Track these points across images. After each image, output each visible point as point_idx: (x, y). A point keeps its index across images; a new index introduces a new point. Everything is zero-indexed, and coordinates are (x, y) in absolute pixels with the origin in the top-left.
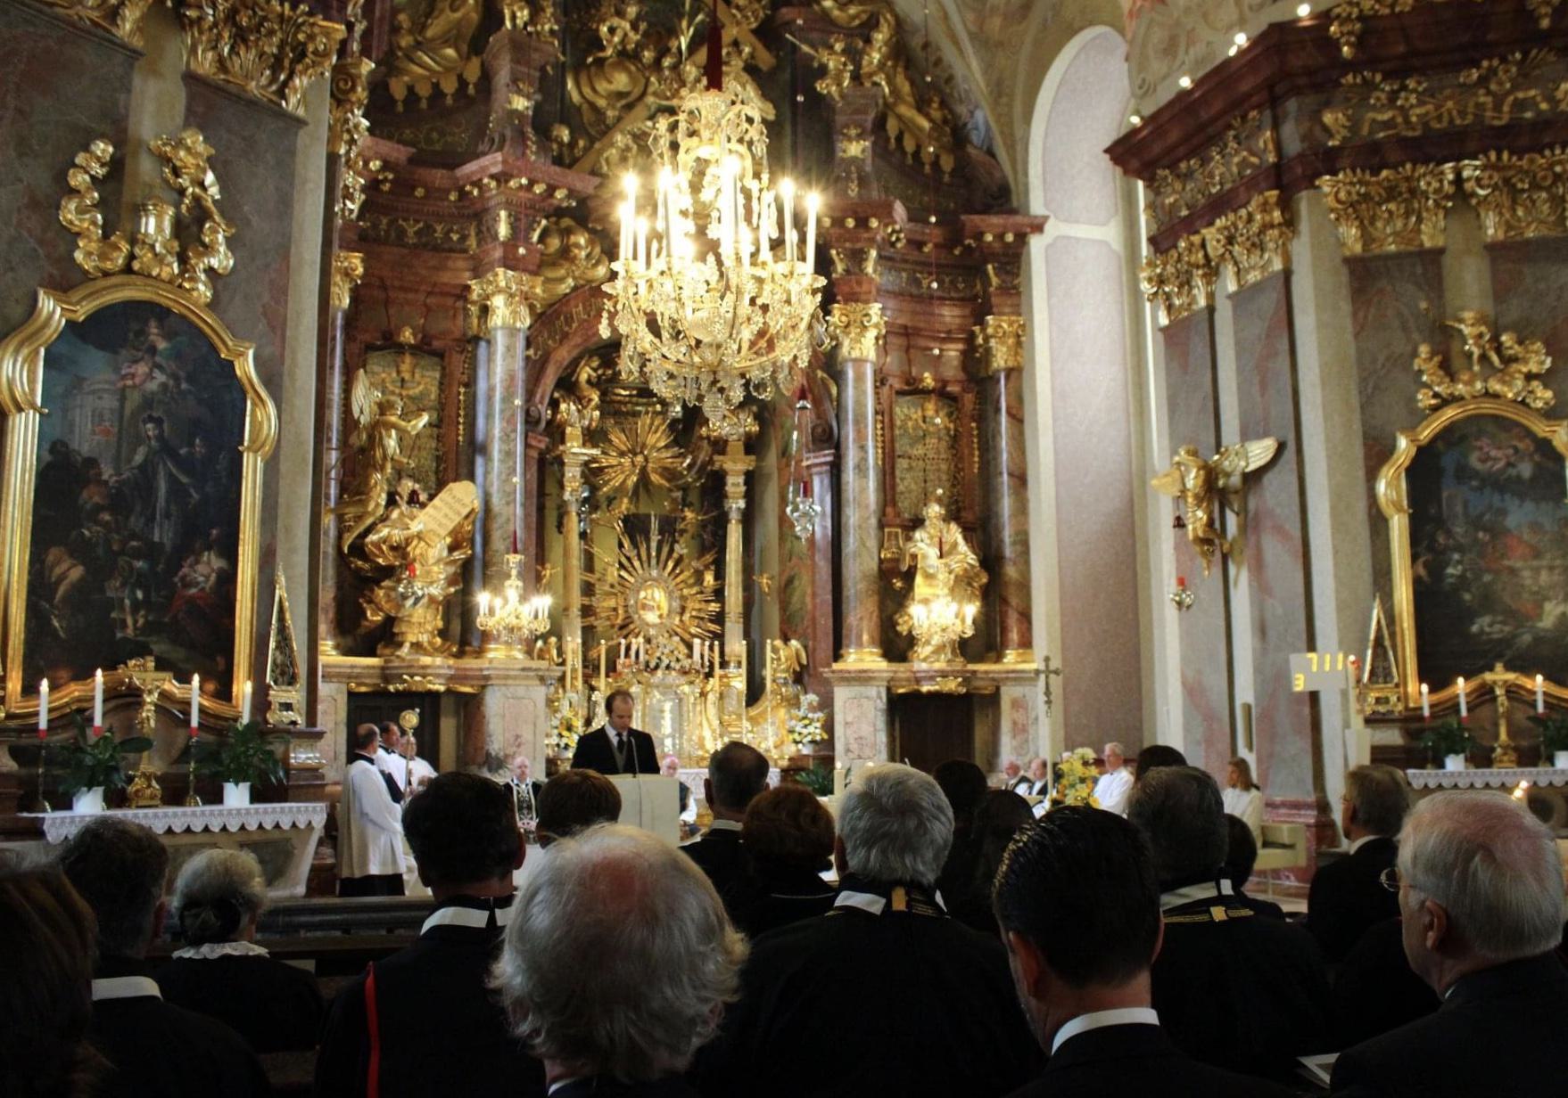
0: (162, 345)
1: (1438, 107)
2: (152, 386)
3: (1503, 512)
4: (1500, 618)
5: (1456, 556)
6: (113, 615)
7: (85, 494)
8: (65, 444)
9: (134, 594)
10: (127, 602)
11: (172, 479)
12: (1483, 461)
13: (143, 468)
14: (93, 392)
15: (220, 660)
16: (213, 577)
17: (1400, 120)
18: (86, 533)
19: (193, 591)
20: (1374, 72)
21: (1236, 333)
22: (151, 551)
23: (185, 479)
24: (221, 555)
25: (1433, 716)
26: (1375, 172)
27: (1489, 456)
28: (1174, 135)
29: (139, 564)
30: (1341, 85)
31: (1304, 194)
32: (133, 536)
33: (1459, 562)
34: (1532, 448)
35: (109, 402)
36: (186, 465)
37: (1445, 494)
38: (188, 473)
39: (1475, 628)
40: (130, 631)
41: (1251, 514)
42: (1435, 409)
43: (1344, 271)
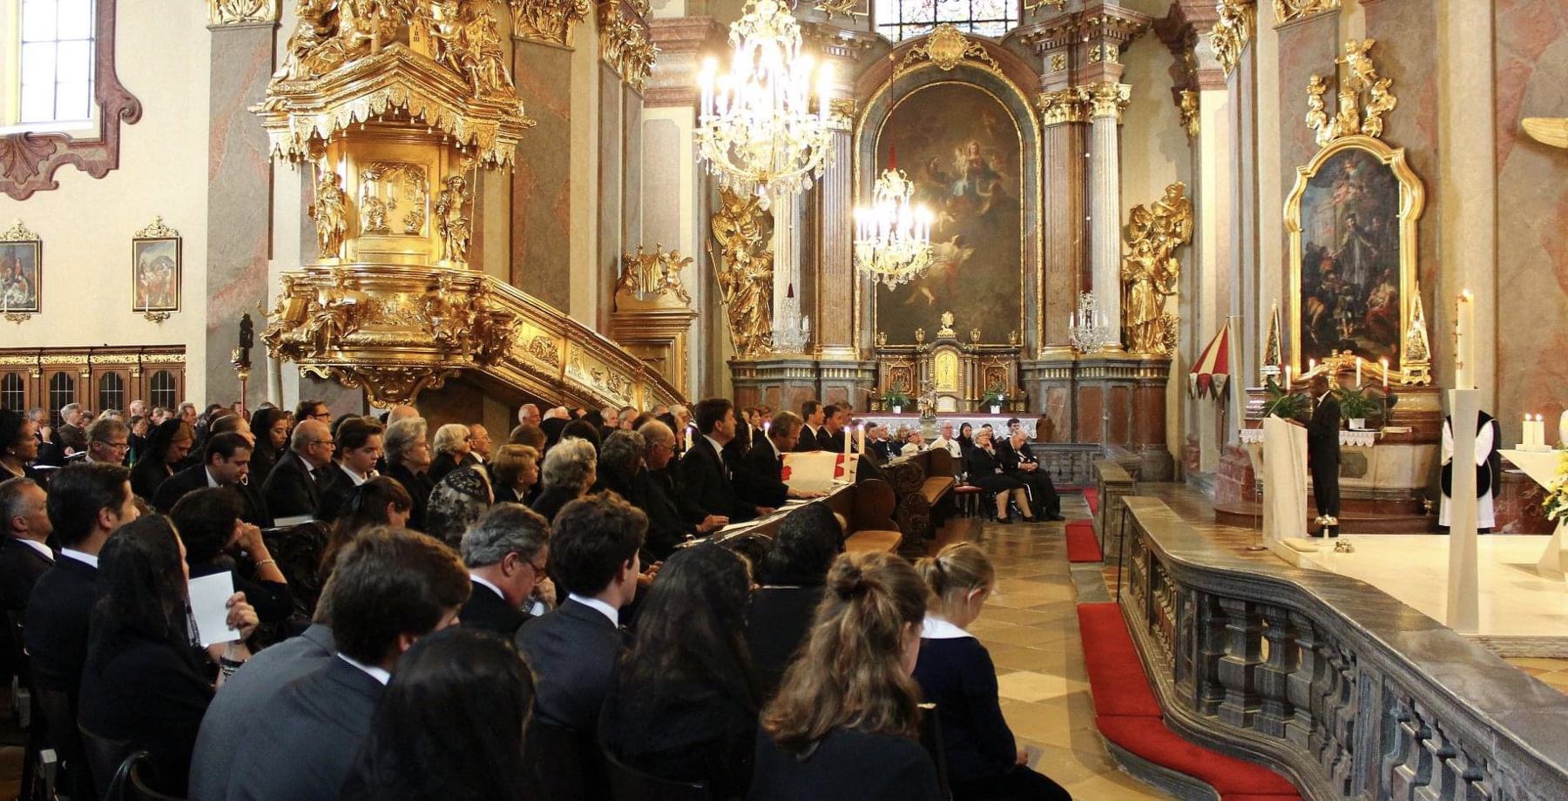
0: (1352, 172)
2: (1350, 197)
6: (1338, 328)
7: (1322, 266)
8: (1311, 243)
9: (1346, 314)
10: (1344, 320)
11: (1364, 249)
13: (1347, 244)
14: (1321, 212)
15: (1393, 347)
16: (1387, 299)
18: (1324, 287)
19: (1376, 308)
22: (1354, 290)
23: (1369, 245)
24: (1392, 284)
29: (1349, 298)
32: (1345, 284)
35: (1329, 214)
36: (1368, 236)
38: (1368, 241)
40: (1346, 335)
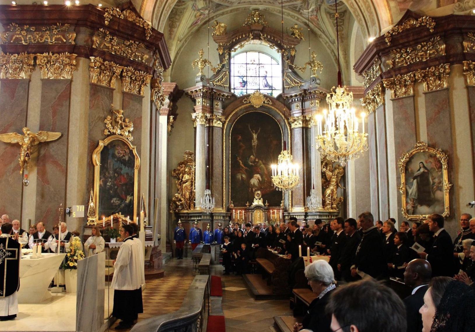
1: (120, 48)
3: (121, 169)
4: (118, 199)
5: (110, 180)
12: (118, 153)
17: (110, 47)
20: (108, 30)
21: (42, 93)
25: (105, 226)
26: (104, 61)
27: (119, 152)
28: (28, 16)
30: (99, 30)
31: (82, 58)
33: (110, 182)
34: (129, 152)
37: (109, 161)
39: (112, 201)
41: (41, 155)
42: (108, 136)
43: (89, 87)
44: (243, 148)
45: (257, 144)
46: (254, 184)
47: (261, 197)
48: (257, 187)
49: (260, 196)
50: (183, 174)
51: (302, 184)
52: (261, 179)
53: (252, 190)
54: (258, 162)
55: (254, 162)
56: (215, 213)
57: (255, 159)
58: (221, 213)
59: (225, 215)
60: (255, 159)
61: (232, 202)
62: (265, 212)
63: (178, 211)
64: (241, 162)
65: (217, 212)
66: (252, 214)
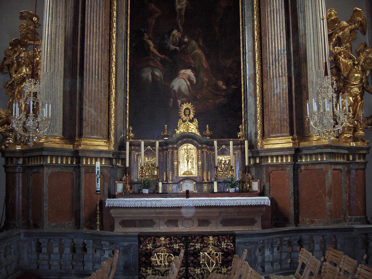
44: (157, 15)
45: (186, 8)
46: (179, 89)
47: (195, 117)
48: (185, 96)
49: (192, 116)
50: (19, 65)
51: (286, 86)
52: (194, 80)
53: (175, 103)
54: (187, 44)
55: (181, 43)
56: (83, 150)
57: (183, 37)
58: (102, 151)
59: (111, 156)
60: (183, 37)
61: (131, 129)
62: (201, 148)
63: (6, 147)
64: (151, 43)
65: (91, 148)
66: (172, 152)
